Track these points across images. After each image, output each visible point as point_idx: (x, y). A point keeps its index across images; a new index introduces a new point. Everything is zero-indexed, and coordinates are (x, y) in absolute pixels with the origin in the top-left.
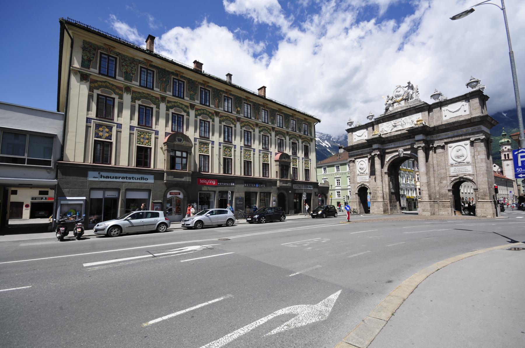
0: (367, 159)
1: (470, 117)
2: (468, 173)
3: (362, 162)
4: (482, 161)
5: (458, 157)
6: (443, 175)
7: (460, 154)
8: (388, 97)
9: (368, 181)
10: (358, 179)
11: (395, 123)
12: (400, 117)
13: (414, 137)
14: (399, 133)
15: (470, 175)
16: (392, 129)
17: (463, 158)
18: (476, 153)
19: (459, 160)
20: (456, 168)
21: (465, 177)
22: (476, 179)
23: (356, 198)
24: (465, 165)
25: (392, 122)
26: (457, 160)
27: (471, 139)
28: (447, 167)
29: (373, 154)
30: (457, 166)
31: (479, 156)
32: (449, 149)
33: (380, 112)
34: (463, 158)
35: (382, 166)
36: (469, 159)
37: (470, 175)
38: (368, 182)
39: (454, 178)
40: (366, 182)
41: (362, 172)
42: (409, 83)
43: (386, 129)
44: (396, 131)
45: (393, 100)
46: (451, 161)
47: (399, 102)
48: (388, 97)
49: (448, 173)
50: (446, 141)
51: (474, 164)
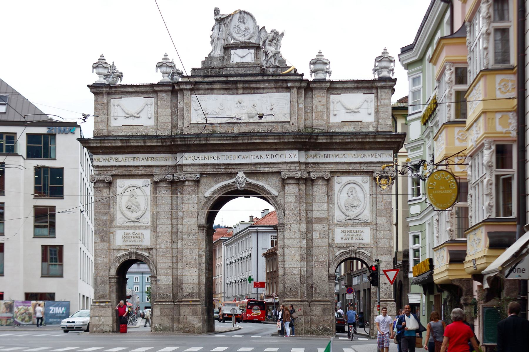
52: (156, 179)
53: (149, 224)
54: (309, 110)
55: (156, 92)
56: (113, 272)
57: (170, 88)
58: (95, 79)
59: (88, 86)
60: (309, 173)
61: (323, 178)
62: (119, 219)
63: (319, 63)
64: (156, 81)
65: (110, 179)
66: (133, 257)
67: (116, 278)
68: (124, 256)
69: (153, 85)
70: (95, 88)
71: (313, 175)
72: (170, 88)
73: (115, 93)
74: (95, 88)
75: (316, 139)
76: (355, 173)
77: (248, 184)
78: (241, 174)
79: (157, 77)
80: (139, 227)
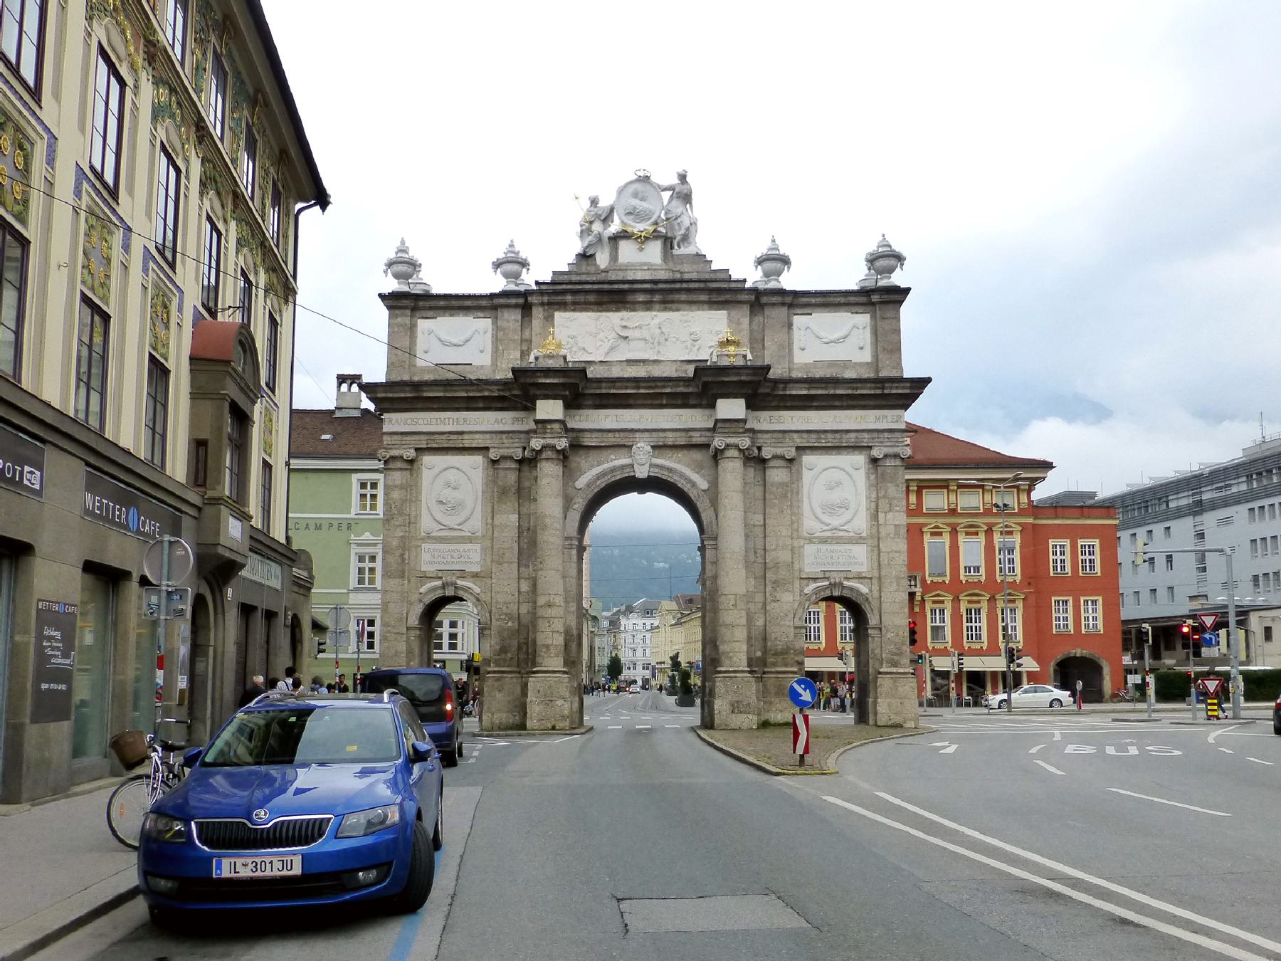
0: (478, 459)
1: (872, 375)
2: (855, 569)
3: (451, 476)
4: (897, 534)
5: (831, 509)
6: (783, 573)
7: (835, 496)
8: (594, 202)
9: (476, 569)
10: (425, 557)
11: (625, 327)
12: (648, 306)
13: (712, 406)
14: (640, 372)
15: (860, 578)
16: (612, 349)
17: (847, 515)
18: (883, 504)
19: (835, 522)
20: (824, 547)
21: (845, 583)
22: (876, 594)
23: (409, 652)
24: (851, 541)
25: (614, 319)
26: (825, 518)
27: (876, 453)
28: (796, 544)
29: (536, 443)
30: (824, 541)
31: (890, 515)
32: (807, 476)
33: (550, 257)
34: (847, 515)
35: (568, 502)
36: (861, 523)
37: (860, 578)
38: (475, 576)
39: (813, 586)
40: (463, 574)
41: (452, 521)
42: (683, 178)
43: (583, 338)
44: (629, 361)
45: (615, 227)
46: (809, 524)
47: (643, 240)
48: (594, 202)
49: (796, 566)
50: (799, 441)
51: (875, 540)
52: (493, 454)
53: (479, 534)
54: (757, 342)
55: (495, 308)
56: (414, 620)
57: (521, 301)
58: (392, 285)
59: (380, 295)
60: (759, 448)
61: (782, 457)
62: (426, 524)
63: (775, 261)
64: (497, 290)
65: (410, 454)
66: (450, 592)
67: (420, 629)
68: (434, 589)
69: (492, 296)
70: (392, 300)
71: (767, 453)
72: (521, 301)
73: (425, 309)
74: (392, 300)
75: (774, 388)
76: (837, 449)
77: (651, 465)
78: (642, 447)
79: (495, 284)
80: (463, 540)
